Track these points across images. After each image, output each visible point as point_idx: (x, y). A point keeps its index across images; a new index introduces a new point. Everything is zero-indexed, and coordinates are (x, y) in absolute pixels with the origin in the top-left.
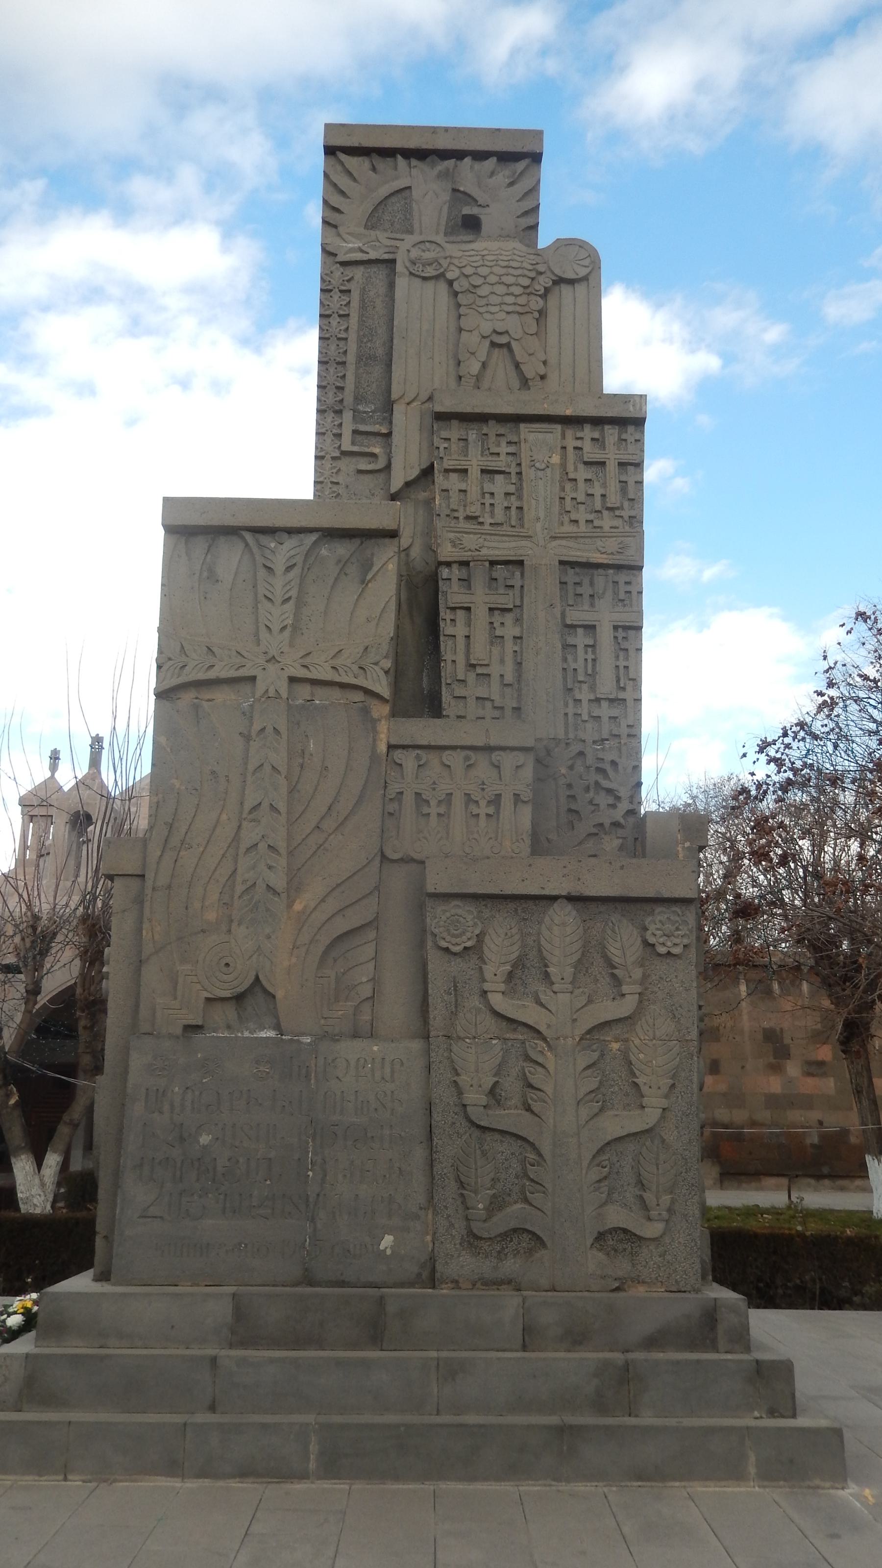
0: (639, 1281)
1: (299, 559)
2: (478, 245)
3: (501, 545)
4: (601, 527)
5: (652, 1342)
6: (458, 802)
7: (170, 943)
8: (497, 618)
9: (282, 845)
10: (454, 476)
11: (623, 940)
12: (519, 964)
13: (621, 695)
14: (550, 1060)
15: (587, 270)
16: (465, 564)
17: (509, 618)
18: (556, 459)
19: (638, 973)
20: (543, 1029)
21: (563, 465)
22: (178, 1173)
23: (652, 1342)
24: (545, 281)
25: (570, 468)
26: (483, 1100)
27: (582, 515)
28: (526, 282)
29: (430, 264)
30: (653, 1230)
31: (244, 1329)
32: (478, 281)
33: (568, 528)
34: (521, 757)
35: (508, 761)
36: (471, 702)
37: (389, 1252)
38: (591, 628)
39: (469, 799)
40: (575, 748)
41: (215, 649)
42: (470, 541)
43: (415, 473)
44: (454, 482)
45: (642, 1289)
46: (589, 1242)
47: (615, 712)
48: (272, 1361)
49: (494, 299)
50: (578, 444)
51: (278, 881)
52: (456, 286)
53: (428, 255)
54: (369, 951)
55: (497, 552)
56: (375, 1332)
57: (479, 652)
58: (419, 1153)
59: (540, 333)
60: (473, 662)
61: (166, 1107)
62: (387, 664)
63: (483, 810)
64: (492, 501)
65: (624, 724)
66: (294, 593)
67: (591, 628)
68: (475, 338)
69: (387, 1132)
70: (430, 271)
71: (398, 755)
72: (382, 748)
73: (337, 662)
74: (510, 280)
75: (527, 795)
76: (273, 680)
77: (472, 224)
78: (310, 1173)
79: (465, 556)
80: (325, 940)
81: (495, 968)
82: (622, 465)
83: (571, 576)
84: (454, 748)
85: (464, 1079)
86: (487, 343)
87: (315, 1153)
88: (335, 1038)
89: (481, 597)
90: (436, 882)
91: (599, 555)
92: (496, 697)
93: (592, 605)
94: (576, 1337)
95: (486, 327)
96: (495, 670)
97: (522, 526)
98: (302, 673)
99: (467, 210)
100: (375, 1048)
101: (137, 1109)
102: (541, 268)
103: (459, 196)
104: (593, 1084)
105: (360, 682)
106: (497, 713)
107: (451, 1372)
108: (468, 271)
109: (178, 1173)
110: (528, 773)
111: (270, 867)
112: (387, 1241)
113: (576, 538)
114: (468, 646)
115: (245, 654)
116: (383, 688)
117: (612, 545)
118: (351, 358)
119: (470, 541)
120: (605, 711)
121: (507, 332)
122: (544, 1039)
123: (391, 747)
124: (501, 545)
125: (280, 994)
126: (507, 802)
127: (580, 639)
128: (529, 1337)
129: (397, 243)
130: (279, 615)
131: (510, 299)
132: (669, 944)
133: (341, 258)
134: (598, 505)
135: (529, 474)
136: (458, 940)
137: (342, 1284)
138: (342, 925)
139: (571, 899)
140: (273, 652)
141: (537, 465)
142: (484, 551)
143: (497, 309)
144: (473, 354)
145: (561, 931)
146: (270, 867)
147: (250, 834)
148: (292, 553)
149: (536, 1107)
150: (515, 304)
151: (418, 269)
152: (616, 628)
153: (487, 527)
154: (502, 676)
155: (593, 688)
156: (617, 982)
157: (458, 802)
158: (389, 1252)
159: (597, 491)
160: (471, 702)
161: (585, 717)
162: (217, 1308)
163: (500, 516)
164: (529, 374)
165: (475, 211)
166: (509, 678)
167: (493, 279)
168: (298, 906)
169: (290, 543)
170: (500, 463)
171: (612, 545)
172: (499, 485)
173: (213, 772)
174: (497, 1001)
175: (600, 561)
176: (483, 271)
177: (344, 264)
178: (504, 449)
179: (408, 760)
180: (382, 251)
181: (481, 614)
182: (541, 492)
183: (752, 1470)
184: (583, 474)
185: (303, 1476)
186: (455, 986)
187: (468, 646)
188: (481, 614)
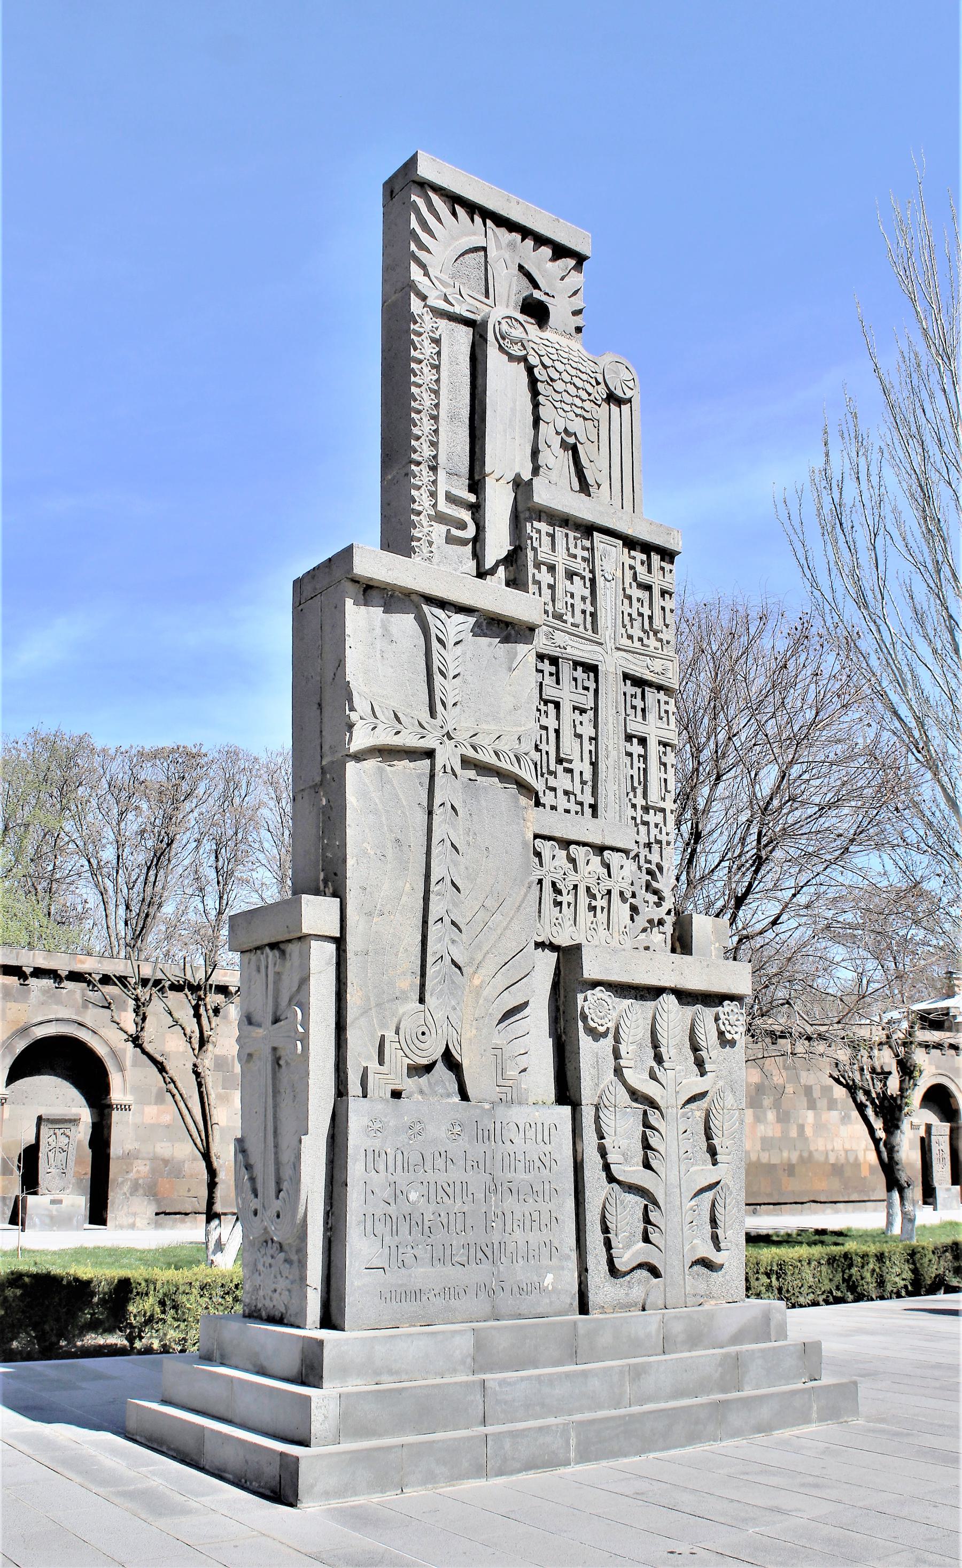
0: (710, 1296)
3: (581, 647)
4: (648, 646)
5: (736, 1339)
7: (370, 1009)
20: (658, 1099)
22: (394, 1227)
23: (736, 1339)
25: (627, 585)
27: (637, 632)
29: (516, 344)
32: (555, 376)
35: (615, 859)
37: (550, 1288)
41: (400, 715)
45: (713, 1302)
48: (522, 1379)
50: (632, 562)
55: (580, 654)
60: (562, 756)
61: (382, 1167)
63: (600, 903)
64: (572, 601)
65: (664, 832)
69: (547, 1187)
70: (517, 351)
73: (500, 746)
78: (494, 1224)
79: (555, 652)
82: (663, 593)
83: (630, 690)
84: (578, 843)
87: (497, 1207)
90: (591, 970)
91: (647, 672)
92: (578, 792)
93: (644, 718)
94: (695, 1339)
96: (576, 766)
97: (595, 630)
98: (471, 753)
100: (537, 1114)
105: (515, 769)
106: (578, 808)
107: (637, 1373)
109: (394, 1227)
111: (453, 942)
113: (634, 653)
114: (558, 737)
115: (425, 725)
117: (657, 665)
121: (575, 434)
122: (658, 1108)
124: (581, 647)
132: (733, 1032)
134: (647, 627)
135: (600, 581)
136: (596, 1019)
137: (520, 1316)
141: (606, 575)
142: (569, 650)
143: (567, 408)
144: (549, 447)
146: (453, 942)
148: (460, 628)
149: (654, 1163)
150: (582, 408)
152: (660, 743)
153: (569, 625)
154: (581, 773)
155: (645, 796)
158: (550, 1288)
159: (646, 611)
161: (639, 821)
164: (591, 481)
166: (588, 776)
169: (460, 618)
170: (580, 566)
171: (657, 665)
173: (398, 840)
175: (650, 678)
178: (580, 553)
180: (465, 307)
183: (814, 1416)
184: (636, 593)
185: (567, 1463)
186: (597, 1062)
187: (558, 737)
188: (566, 708)
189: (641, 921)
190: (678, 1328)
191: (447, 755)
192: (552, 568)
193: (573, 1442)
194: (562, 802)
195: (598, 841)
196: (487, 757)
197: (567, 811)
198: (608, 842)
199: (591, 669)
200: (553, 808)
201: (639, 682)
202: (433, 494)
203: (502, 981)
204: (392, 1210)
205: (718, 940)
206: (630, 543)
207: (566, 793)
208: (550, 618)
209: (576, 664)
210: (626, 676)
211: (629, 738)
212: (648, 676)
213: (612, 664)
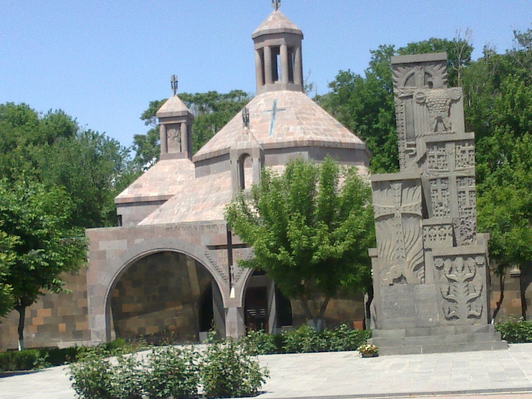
1: (401, 187)
2: (432, 91)
6: (437, 235)
8: (443, 191)
9: (404, 248)
10: (431, 158)
11: (471, 262)
12: (451, 269)
13: (471, 207)
14: (458, 285)
15: (459, 97)
16: (435, 180)
17: (446, 191)
18: (454, 151)
19: (474, 268)
21: (455, 152)
23: (478, 331)
24: (449, 101)
26: (446, 294)
28: (444, 102)
30: (478, 314)
31: (407, 334)
32: (433, 103)
33: (458, 168)
34: (449, 226)
35: (447, 227)
36: (439, 211)
38: (464, 192)
39: (440, 235)
40: (462, 220)
42: (436, 173)
43: (422, 155)
44: (432, 159)
45: (477, 324)
46: (467, 316)
47: (470, 211)
49: (437, 108)
51: (404, 256)
52: (428, 105)
53: (421, 96)
54: (423, 267)
56: (430, 333)
57: (440, 199)
58: (436, 304)
59: (449, 116)
62: (421, 208)
63: (443, 237)
66: (400, 194)
67: (464, 192)
68: (434, 118)
70: (422, 101)
71: (425, 228)
72: (421, 226)
74: (440, 102)
75: (451, 233)
76: (398, 214)
77: (431, 84)
79: (435, 177)
80: (414, 266)
81: (447, 269)
83: (459, 180)
85: (443, 290)
86: (436, 121)
88: (418, 284)
89: (439, 186)
94: (464, 332)
95: (436, 116)
96: (444, 203)
98: (404, 212)
99: (430, 80)
101: (383, 300)
102: (448, 97)
103: (426, 73)
104: (466, 289)
107: (443, 338)
108: (431, 100)
110: (451, 229)
112: (431, 319)
116: (420, 214)
117: (468, 171)
118: (404, 125)
119: (436, 173)
120: (468, 211)
123: (423, 226)
125: (406, 277)
126: (447, 235)
127: (462, 195)
128: (456, 332)
129: (413, 90)
130: (398, 199)
131: (441, 108)
133: (399, 96)
138: (417, 263)
139: (461, 255)
140: (397, 208)
145: (459, 261)
147: (398, 246)
149: (456, 294)
151: (418, 101)
156: (470, 271)
157: (437, 235)
159: (464, 157)
160: (439, 211)
162: (403, 331)
163: (442, 166)
164: (447, 127)
165: (431, 80)
167: (436, 102)
168: (407, 260)
171: (468, 171)
172: (442, 158)
174: (447, 275)
176: (434, 100)
177: (401, 98)
179: (427, 228)
181: (440, 191)
182: (451, 160)
183: (492, 348)
185: (420, 353)
188: (440, 191)
189: (464, 237)
190: (459, 329)
191: (398, 214)
192: (433, 157)
193: (422, 349)
194: (439, 213)
195: (441, 223)
196: (408, 211)
197: (441, 215)
198: (444, 223)
199: (446, 178)
200: (437, 215)
201: (462, 178)
202: (404, 146)
203: (416, 258)
204: (391, 307)
205: (485, 238)
206: (457, 142)
207: (441, 211)
208: (434, 169)
209: (442, 179)
210: (458, 177)
211: (460, 193)
212: (464, 175)
213: (453, 175)
